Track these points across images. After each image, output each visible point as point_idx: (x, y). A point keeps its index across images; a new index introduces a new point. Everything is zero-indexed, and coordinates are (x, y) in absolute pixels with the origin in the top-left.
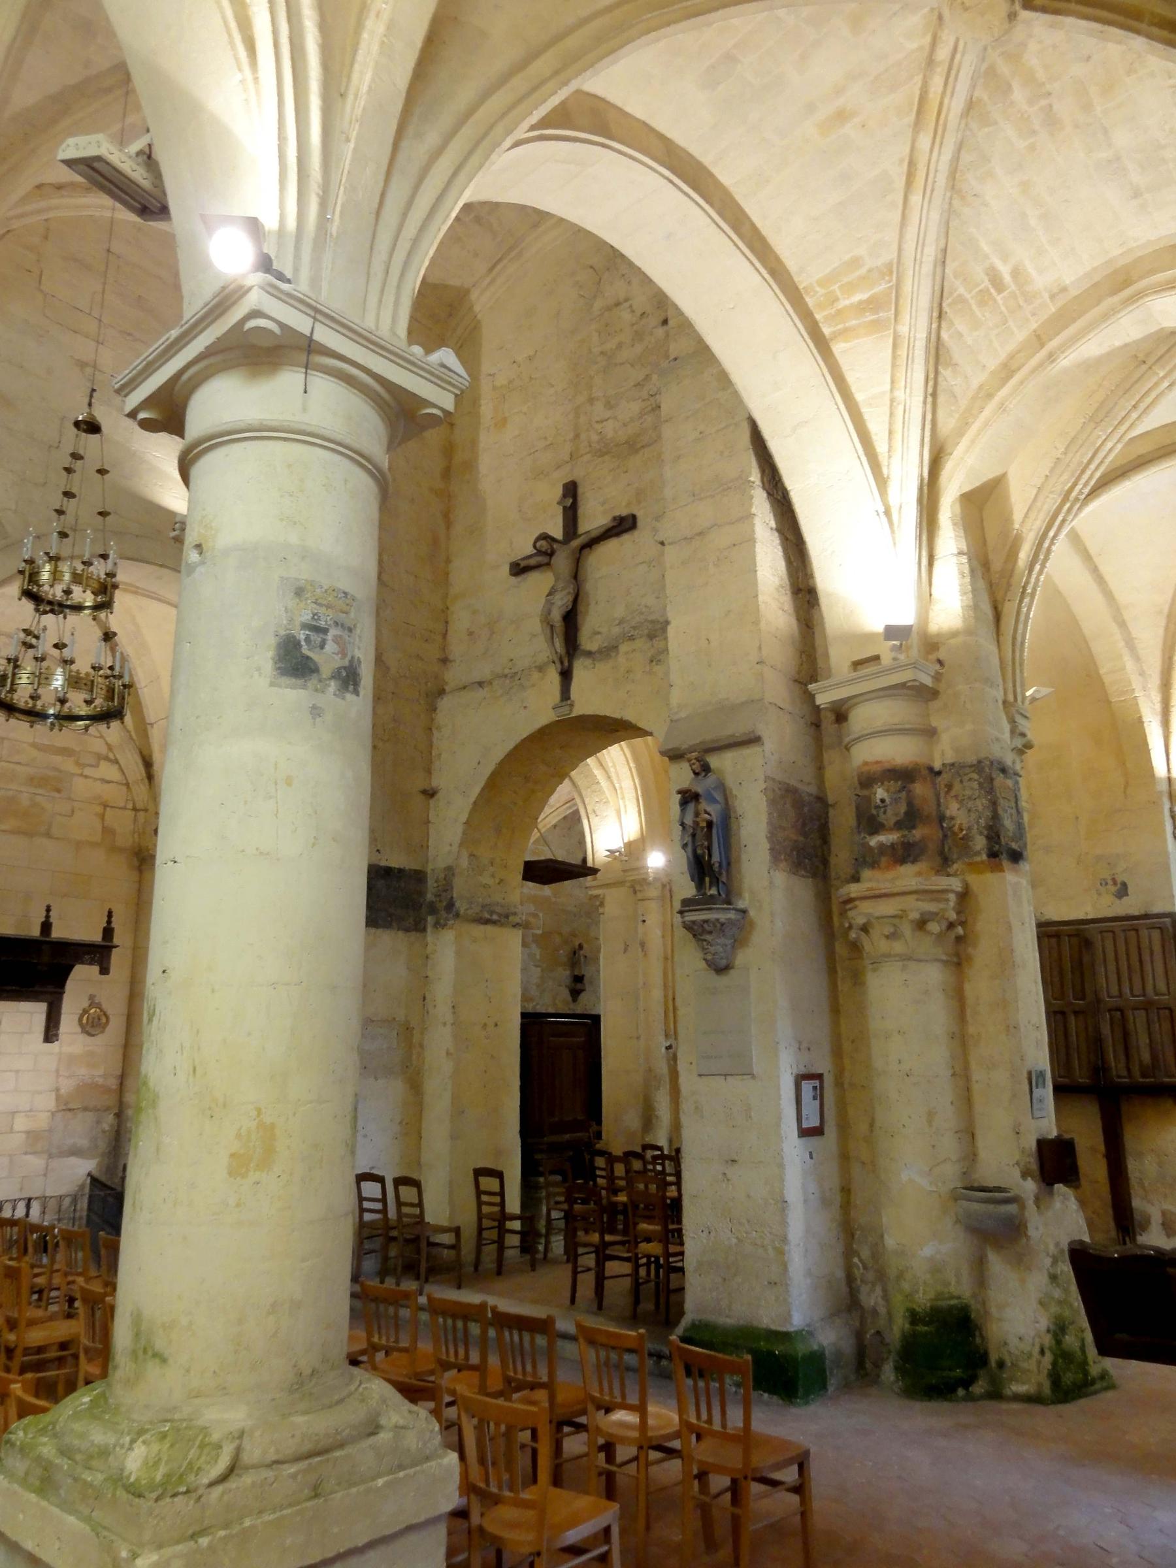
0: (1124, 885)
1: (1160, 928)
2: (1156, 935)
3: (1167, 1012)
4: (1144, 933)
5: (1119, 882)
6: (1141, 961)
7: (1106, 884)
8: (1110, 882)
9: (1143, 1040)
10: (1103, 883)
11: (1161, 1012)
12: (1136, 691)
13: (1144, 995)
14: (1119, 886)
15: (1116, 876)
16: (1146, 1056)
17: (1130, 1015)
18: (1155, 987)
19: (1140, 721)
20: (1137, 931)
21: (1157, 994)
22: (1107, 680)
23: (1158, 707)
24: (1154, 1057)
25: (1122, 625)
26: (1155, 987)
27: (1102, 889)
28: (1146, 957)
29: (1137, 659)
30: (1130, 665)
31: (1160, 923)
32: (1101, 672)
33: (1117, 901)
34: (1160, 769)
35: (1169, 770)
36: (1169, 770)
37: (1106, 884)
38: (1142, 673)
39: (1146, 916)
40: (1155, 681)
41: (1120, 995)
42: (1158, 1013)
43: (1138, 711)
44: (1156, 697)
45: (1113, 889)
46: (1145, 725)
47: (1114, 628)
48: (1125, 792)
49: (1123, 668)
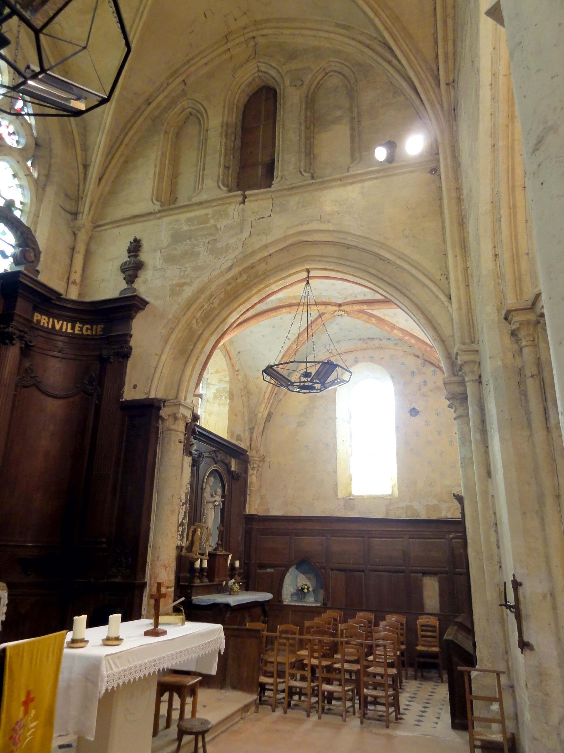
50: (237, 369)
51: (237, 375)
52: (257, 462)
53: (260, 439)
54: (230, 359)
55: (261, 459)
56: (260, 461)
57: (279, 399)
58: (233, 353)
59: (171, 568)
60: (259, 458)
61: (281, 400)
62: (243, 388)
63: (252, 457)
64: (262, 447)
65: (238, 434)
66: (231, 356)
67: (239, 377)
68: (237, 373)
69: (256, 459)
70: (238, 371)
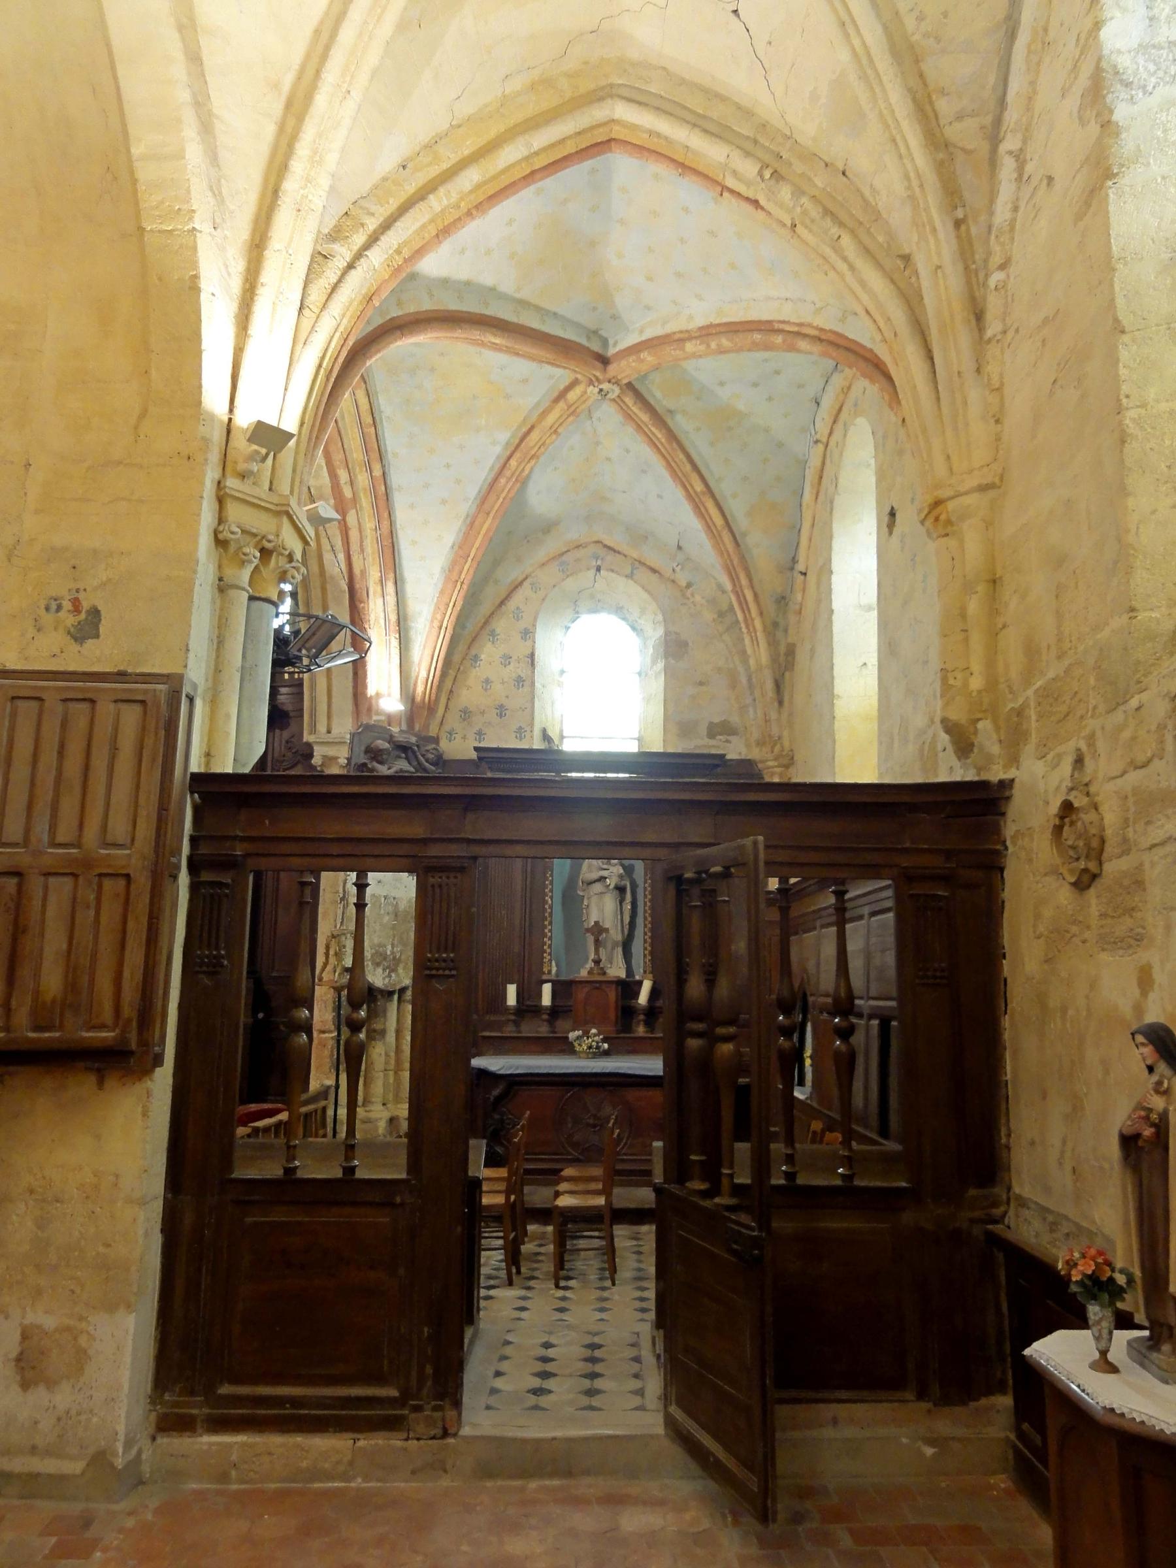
0: (95, 613)
1: (143, 702)
2: (131, 716)
3: (122, 882)
4: (106, 709)
5: (86, 605)
6: (87, 768)
7: (59, 608)
8: (67, 605)
9: (54, 942)
10: (54, 606)
11: (108, 884)
12: (197, 217)
13: (78, 845)
14: (83, 616)
15: (81, 596)
16: (52, 982)
17: (35, 884)
18: (104, 828)
19: (193, 287)
20: (92, 702)
21: (107, 845)
22: (146, 173)
23: (236, 285)
24: (71, 985)
25: (195, 58)
26: (104, 828)
27: (48, 619)
28: (99, 763)
29: (213, 157)
30: (194, 153)
31: (146, 691)
32: (136, 151)
33: (74, 647)
34: (214, 399)
35: (231, 411)
36: (231, 411)
37: (59, 608)
38: (216, 191)
39: (121, 676)
40: (240, 230)
41: (26, 842)
42: (100, 886)
43: (195, 264)
44: (238, 266)
45: (70, 620)
46: (204, 297)
47: (173, 45)
48: (136, 428)
49: (180, 155)
50: (684, 584)
51: (693, 595)
52: (778, 770)
53: (773, 715)
54: (654, 571)
55: (785, 761)
56: (787, 767)
57: (797, 607)
58: (654, 560)
59: (325, 1003)
60: (775, 759)
61: (801, 604)
62: (715, 616)
63: (762, 762)
64: (786, 733)
65: (716, 720)
66: (652, 565)
67: (698, 598)
68: (689, 591)
69: (771, 763)
70: (689, 585)
